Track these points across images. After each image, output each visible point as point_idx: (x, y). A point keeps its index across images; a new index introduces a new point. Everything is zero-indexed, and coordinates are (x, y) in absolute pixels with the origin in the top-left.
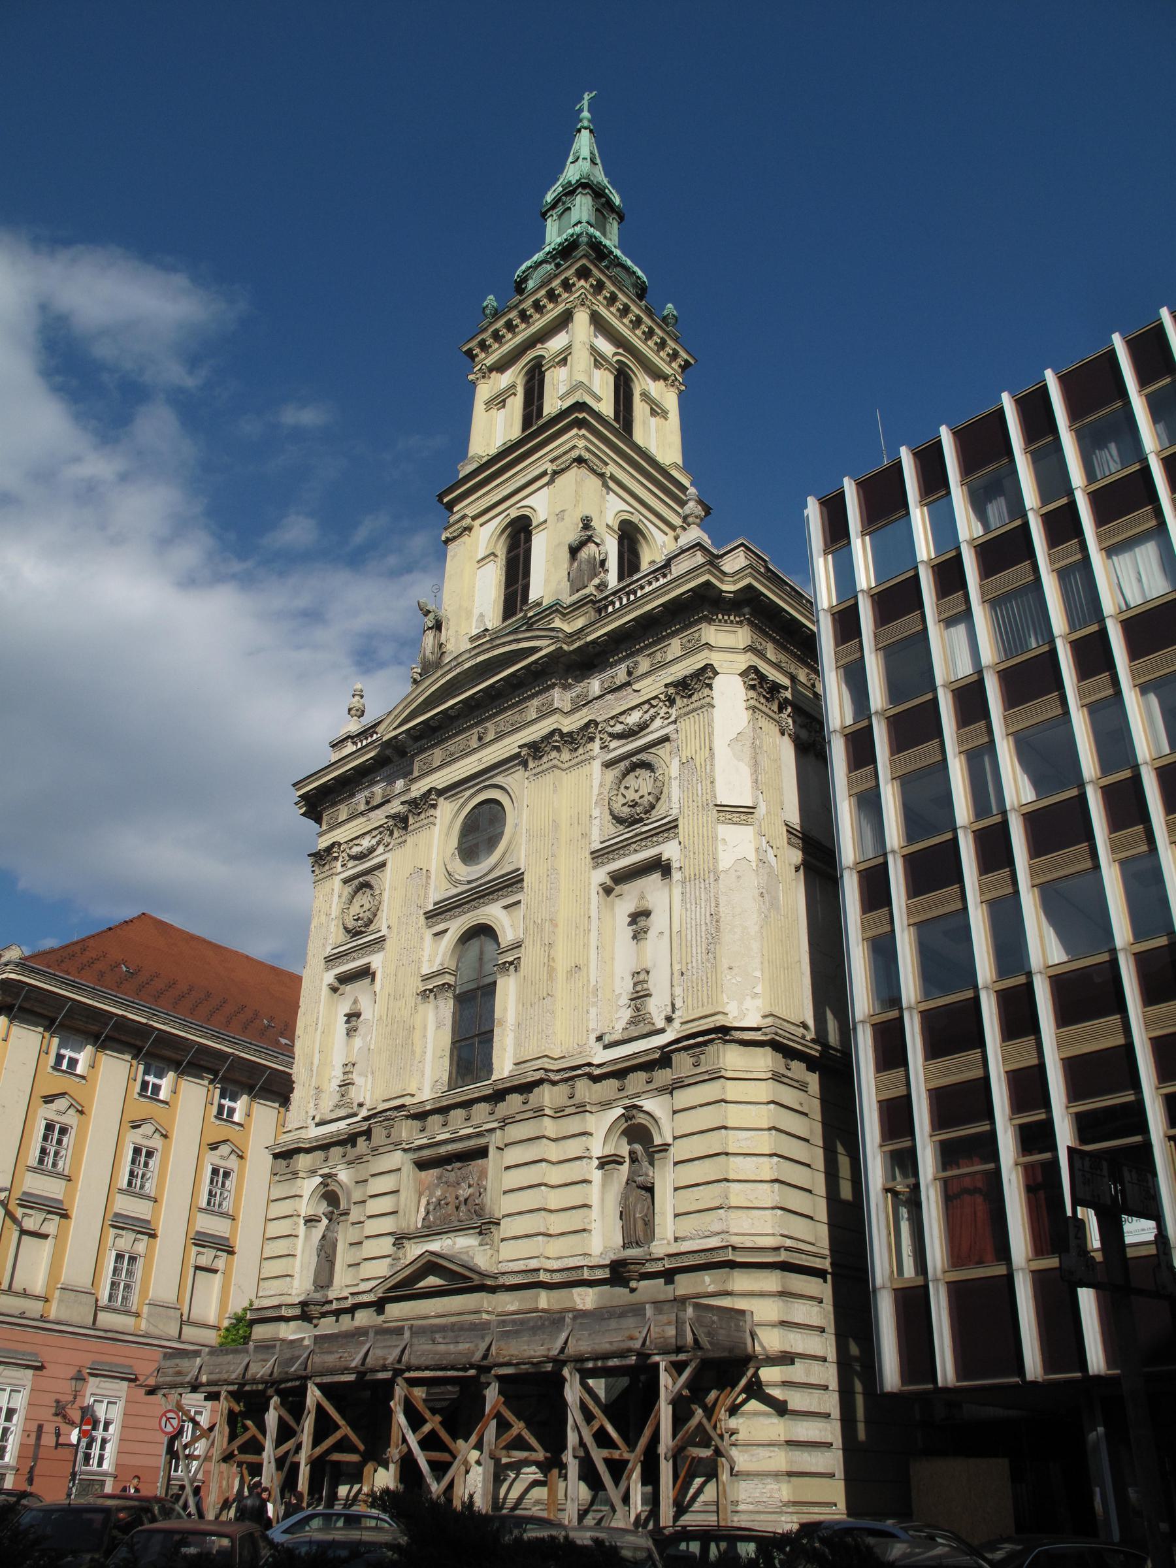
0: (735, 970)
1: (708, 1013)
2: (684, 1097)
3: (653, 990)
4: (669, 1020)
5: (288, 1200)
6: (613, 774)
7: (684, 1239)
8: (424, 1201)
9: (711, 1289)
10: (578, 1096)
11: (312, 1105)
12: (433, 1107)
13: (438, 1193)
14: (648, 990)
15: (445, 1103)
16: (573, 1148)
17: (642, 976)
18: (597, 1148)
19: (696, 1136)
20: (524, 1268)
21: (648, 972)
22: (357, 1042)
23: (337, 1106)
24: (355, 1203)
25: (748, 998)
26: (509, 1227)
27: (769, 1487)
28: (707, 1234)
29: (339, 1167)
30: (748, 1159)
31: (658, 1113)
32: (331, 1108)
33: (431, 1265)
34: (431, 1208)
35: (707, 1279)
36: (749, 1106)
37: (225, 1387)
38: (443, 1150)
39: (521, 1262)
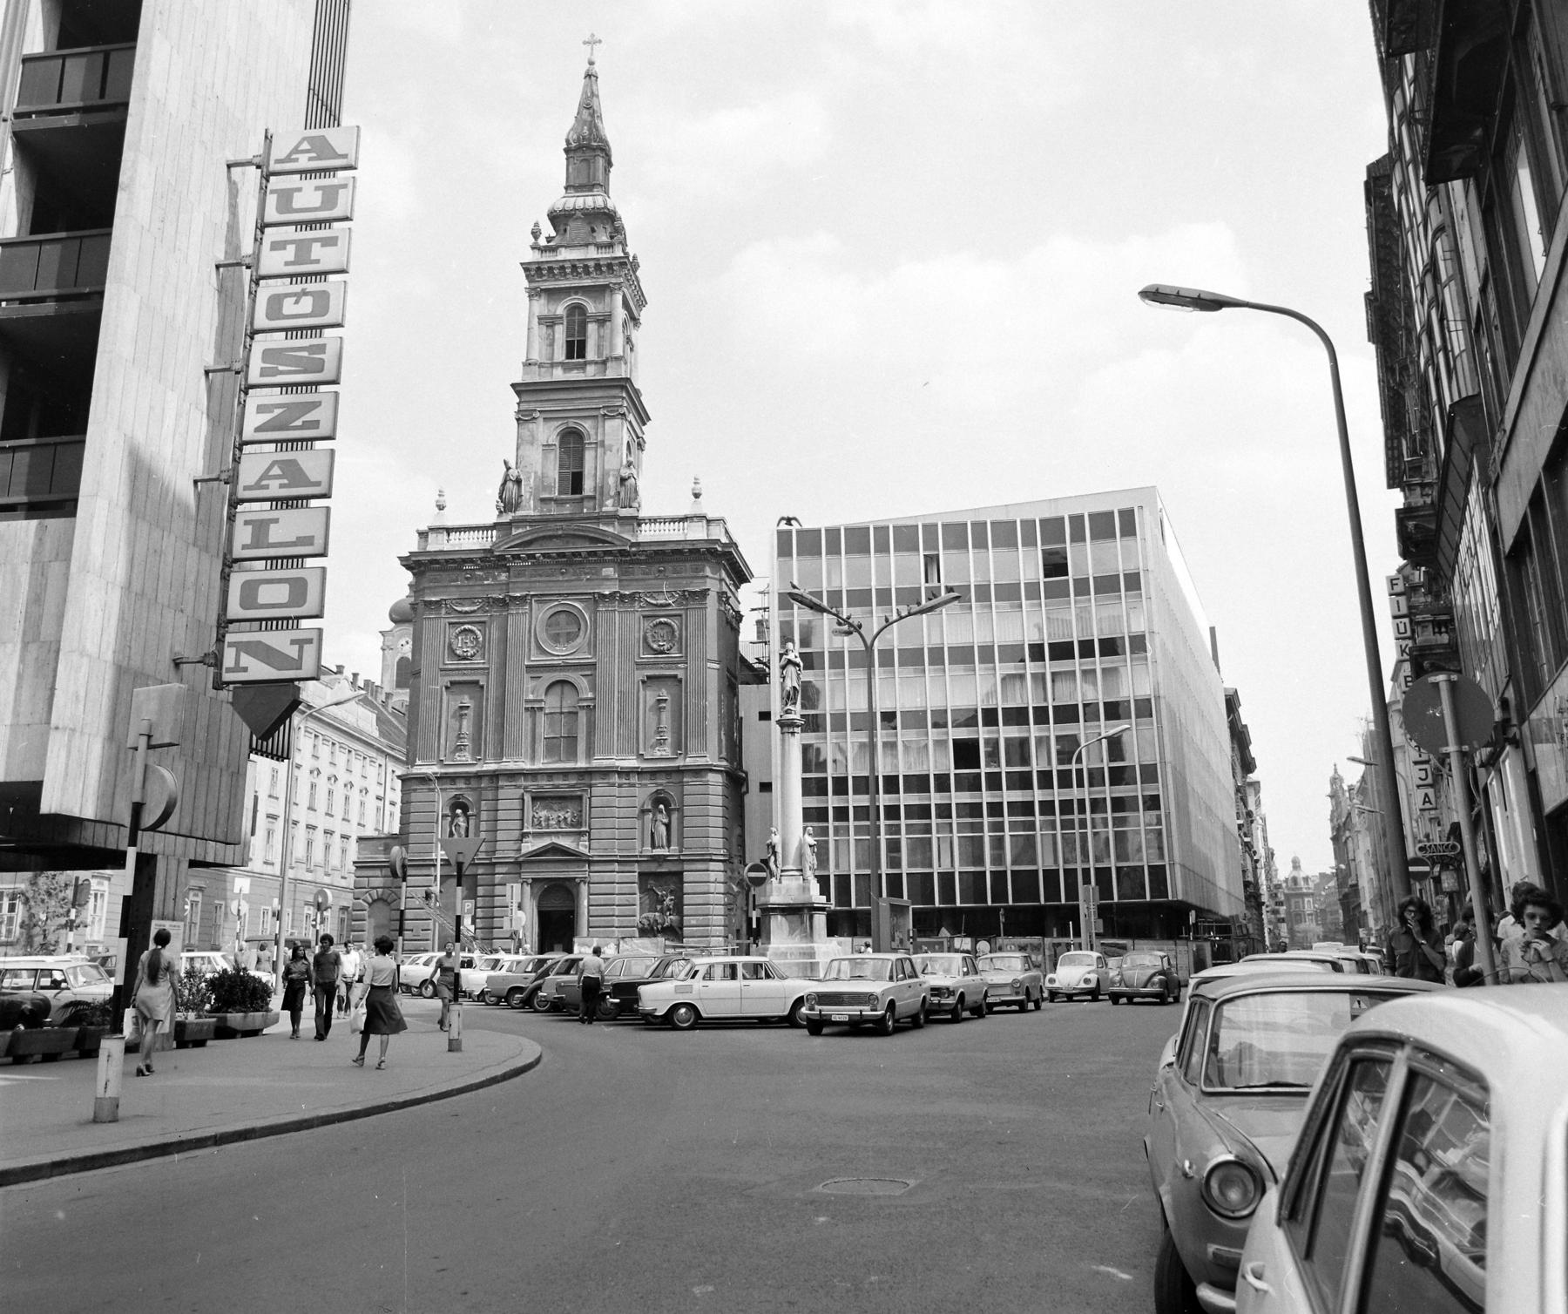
6: (648, 624)
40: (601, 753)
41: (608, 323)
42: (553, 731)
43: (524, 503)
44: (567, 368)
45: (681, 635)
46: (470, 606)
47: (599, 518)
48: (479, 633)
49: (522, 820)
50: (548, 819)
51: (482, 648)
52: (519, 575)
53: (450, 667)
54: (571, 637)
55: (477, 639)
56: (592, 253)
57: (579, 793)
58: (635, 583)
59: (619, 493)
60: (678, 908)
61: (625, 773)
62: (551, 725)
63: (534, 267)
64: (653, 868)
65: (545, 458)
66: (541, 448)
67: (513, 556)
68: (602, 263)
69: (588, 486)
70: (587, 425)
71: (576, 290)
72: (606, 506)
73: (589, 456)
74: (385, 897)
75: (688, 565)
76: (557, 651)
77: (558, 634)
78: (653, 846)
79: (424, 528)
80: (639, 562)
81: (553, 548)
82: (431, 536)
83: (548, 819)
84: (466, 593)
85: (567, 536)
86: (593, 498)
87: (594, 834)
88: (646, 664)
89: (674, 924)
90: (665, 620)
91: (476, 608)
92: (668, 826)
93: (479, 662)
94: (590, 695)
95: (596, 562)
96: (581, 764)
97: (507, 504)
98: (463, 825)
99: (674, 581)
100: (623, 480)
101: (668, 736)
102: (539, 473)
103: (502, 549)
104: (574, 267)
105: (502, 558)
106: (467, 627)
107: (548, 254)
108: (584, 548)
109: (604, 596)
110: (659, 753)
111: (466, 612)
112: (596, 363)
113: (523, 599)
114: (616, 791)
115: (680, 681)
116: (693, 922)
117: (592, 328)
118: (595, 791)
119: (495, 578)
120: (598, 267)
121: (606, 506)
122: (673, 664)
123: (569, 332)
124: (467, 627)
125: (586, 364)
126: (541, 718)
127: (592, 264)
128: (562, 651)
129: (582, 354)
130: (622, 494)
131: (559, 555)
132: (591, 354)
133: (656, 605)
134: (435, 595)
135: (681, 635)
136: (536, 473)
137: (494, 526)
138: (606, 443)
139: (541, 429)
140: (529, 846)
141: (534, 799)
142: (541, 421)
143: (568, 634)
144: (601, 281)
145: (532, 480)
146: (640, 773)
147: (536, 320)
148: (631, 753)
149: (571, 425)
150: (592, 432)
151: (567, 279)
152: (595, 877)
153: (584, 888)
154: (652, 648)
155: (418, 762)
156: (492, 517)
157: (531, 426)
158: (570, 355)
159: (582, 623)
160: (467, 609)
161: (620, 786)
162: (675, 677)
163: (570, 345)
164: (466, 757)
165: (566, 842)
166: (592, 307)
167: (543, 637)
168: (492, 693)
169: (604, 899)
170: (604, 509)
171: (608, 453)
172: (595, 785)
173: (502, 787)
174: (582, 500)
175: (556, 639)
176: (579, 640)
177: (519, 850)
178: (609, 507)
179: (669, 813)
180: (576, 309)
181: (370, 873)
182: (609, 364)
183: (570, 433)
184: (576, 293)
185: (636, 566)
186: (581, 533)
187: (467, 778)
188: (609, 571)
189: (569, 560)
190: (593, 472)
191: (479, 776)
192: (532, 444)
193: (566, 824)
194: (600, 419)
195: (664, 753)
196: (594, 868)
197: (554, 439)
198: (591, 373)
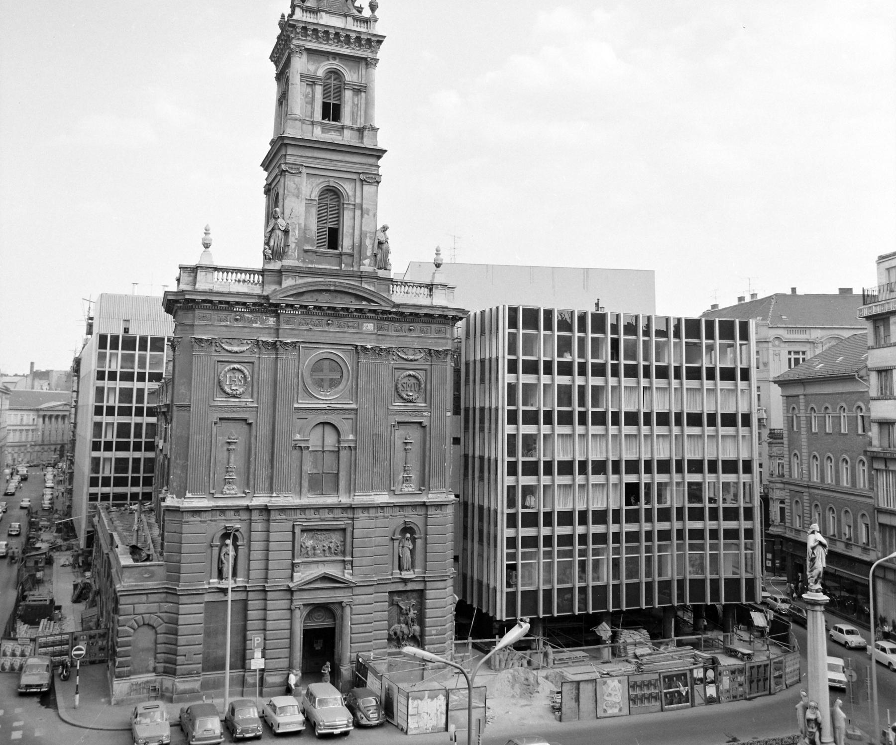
40: (361, 489)
41: (363, 94)
42: (316, 468)
43: (290, 253)
44: (325, 129)
45: (426, 386)
46: (238, 345)
47: (361, 276)
48: (245, 371)
49: (293, 550)
50: (314, 548)
51: (251, 384)
52: (287, 322)
53: (219, 404)
54: (333, 383)
55: (245, 377)
56: (350, 24)
57: (343, 527)
58: (389, 338)
59: (376, 255)
60: (421, 619)
61: (382, 507)
62: (315, 463)
63: (301, 25)
64: (401, 587)
65: (307, 211)
66: (305, 201)
67: (287, 305)
68: (362, 37)
69: (346, 244)
70: (347, 188)
71: (335, 55)
72: (364, 265)
73: (347, 215)
74: (151, 623)
75: (433, 326)
76: (321, 395)
77: (322, 380)
78: (400, 568)
79: (192, 263)
80: (393, 320)
81: (325, 301)
82: (201, 275)
83: (314, 548)
84: (236, 334)
85: (335, 291)
86: (351, 255)
87: (356, 562)
88: (397, 411)
89: (417, 634)
90: (414, 373)
91: (245, 348)
92: (412, 552)
93: (247, 400)
94: (351, 437)
95: (359, 317)
96: (345, 500)
97: (274, 253)
98: (232, 553)
99: (421, 340)
100: (380, 243)
101: (414, 476)
102: (303, 226)
103: (278, 298)
104: (337, 34)
105: (277, 305)
106: (236, 366)
107: (308, 15)
108: (354, 305)
109: (366, 348)
110: (406, 489)
111: (236, 352)
112: (352, 129)
113: (294, 345)
114: (372, 523)
115: (424, 427)
116: (434, 632)
117: (348, 94)
119: (263, 322)
120: (358, 39)
121: (364, 265)
122: (420, 412)
123: (326, 93)
124: (236, 366)
125: (343, 128)
126: (308, 458)
127: (353, 35)
128: (326, 395)
129: (337, 117)
130: (379, 256)
131: (329, 308)
132: (346, 119)
133: (406, 360)
134: (205, 334)
135: (426, 386)
136: (299, 224)
137: (262, 272)
138: (364, 206)
139: (304, 184)
140: (300, 576)
141: (302, 531)
142: (304, 176)
143: (331, 379)
144: (359, 53)
145: (297, 232)
146: (393, 506)
147: (299, 77)
148: (384, 489)
149: (331, 184)
150: (351, 193)
151: (329, 44)
152: (358, 599)
153: (348, 610)
154: (402, 398)
155: (188, 495)
156: (259, 265)
157: (297, 179)
158: (325, 115)
159: (345, 371)
160: (236, 349)
161: (377, 518)
162: (420, 423)
163: (326, 106)
164: (234, 490)
165: (334, 571)
166: (350, 76)
167: (308, 381)
168: (263, 430)
169: (365, 618)
170: (362, 268)
171: (365, 216)
173: (274, 521)
174: (341, 255)
175: (320, 383)
176: (341, 387)
177: (292, 578)
178: (367, 266)
179: (413, 540)
180: (334, 73)
181: (135, 599)
182: (366, 133)
183: (327, 190)
184: (335, 59)
185: (391, 324)
186: (350, 291)
187: (237, 510)
188: (369, 326)
189: (335, 313)
190: (351, 231)
191: (248, 509)
192: (298, 197)
193: (331, 553)
194: (358, 184)
195: (410, 489)
196: (357, 591)
197: (315, 195)
198: (348, 138)
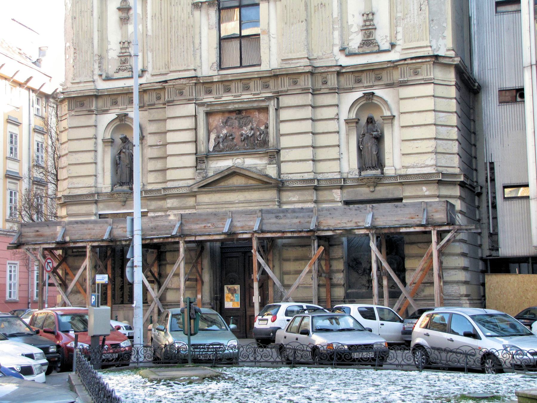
0: (435, 22)
1: (422, 45)
2: (405, 92)
3: (377, 26)
4: (393, 46)
5: (86, 128)
7: (407, 167)
8: (213, 136)
9: (427, 193)
10: (329, 83)
11: (96, 66)
12: (220, 80)
13: (225, 131)
14: (374, 25)
15: (230, 79)
16: (330, 113)
17: (370, 17)
18: (344, 116)
19: (415, 113)
20: (301, 178)
21: (373, 14)
22: (131, 28)
23: (119, 70)
24: (150, 134)
25: (441, 38)
26: (284, 155)
27: (454, 288)
28: (422, 165)
29: (128, 110)
30: (443, 128)
31: (386, 98)
32: (115, 70)
33: (232, 173)
34: (221, 140)
35: (424, 188)
36: (444, 100)
37: (90, 244)
38: (231, 107)
39: (299, 175)
118: (285, 101)
172: (286, 93)
